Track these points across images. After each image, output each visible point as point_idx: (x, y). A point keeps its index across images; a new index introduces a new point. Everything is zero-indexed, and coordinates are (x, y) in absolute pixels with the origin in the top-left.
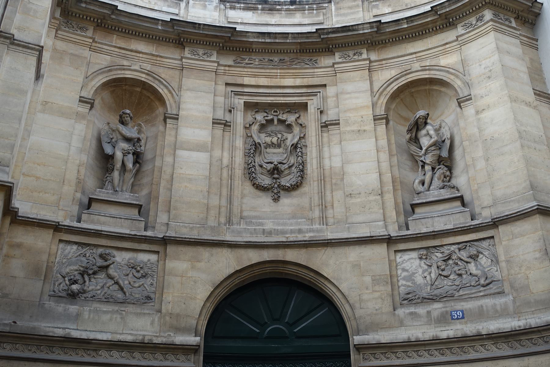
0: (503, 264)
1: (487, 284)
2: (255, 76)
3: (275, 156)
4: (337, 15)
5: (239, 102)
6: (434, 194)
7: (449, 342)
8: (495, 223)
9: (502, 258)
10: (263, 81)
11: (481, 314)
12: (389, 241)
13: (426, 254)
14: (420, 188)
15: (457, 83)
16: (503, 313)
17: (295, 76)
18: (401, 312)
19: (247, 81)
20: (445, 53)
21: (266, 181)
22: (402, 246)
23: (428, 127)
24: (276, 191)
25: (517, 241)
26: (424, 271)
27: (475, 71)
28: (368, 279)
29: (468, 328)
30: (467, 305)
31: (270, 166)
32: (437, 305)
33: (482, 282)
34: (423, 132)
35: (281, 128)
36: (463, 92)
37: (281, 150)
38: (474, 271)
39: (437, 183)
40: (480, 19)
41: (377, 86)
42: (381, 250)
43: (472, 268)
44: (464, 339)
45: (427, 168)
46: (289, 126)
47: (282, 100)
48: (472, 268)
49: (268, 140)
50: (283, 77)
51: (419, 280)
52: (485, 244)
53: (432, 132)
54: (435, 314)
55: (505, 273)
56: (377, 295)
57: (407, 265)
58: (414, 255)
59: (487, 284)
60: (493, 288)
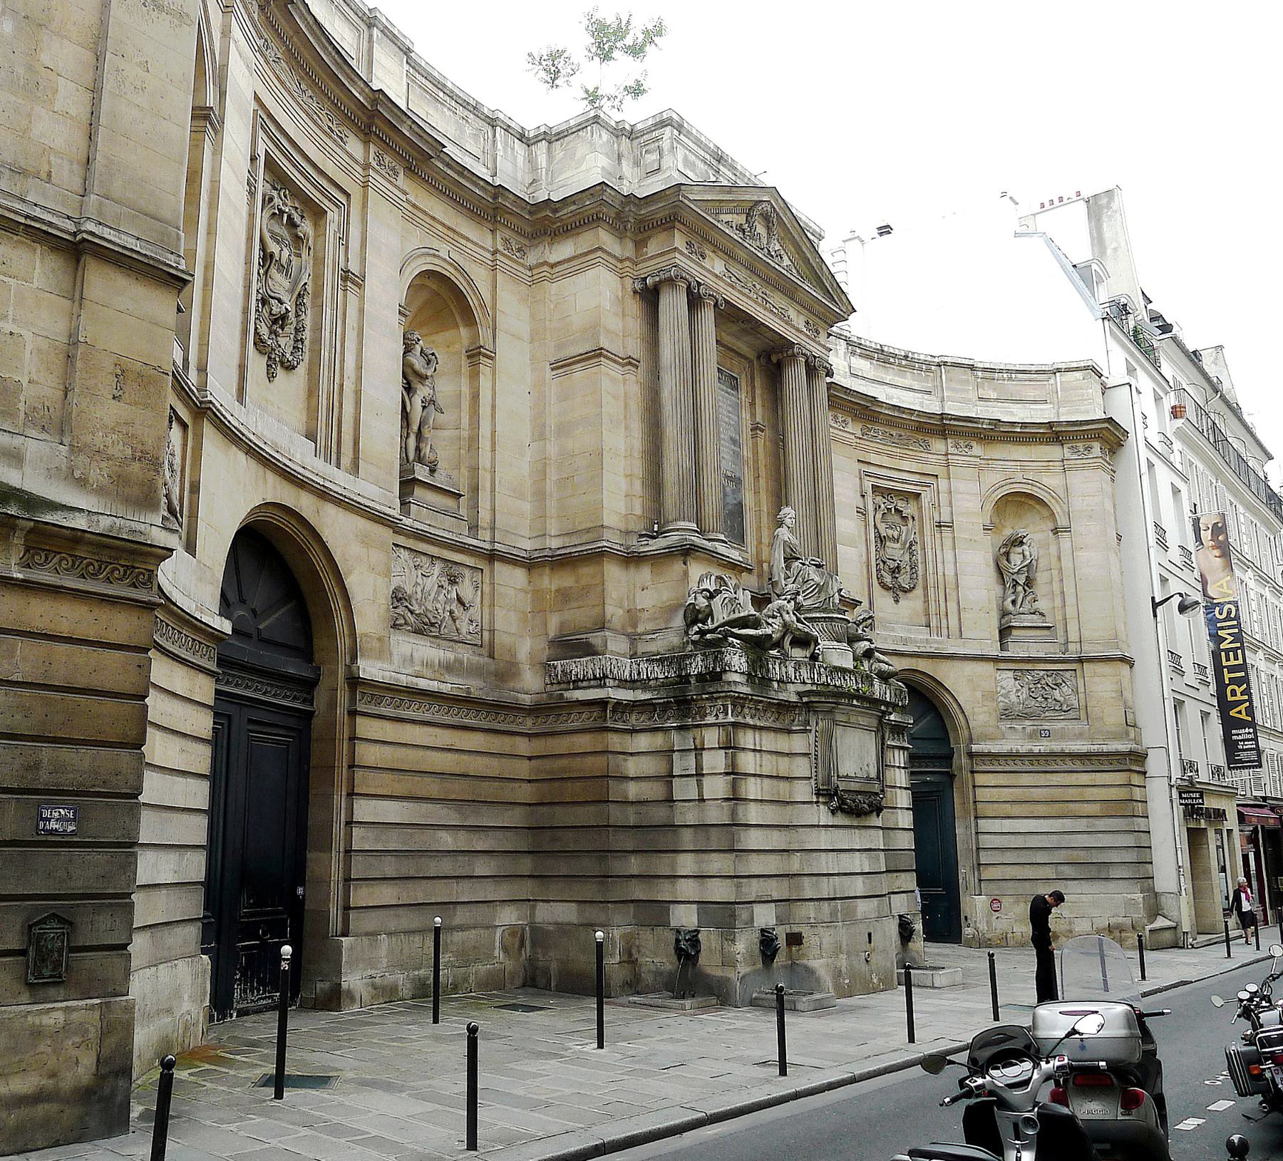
0: (1082, 696)
1: (1064, 710)
2: (878, 453)
3: (894, 550)
4: (948, 389)
5: (868, 485)
6: (1028, 620)
7: (1040, 755)
8: (1081, 661)
9: (1081, 690)
10: (886, 461)
11: (1063, 736)
12: (996, 660)
13: (1018, 675)
14: (1010, 607)
15: (1056, 509)
16: (1080, 736)
17: (913, 458)
18: (1004, 726)
19: (873, 458)
20: (1047, 469)
21: (888, 579)
22: (1003, 666)
23: (1025, 547)
24: (898, 592)
25: (1097, 679)
26: (1018, 691)
27: (1077, 504)
28: (979, 694)
29: (1056, 746)
30: (1047, 725)
31: (893, 565)
32: (1028, 723)
33: (1065, 708)
34: (1019, 550)
35: (897, 519)
36: (1062, 522)
37: (898, 545)
38: (1059, 698)
39: (1026, 607)
40: (1089, 449)
41: (984, 489)
42: (989, 668)
43: (1057, 694)
44: (1052, 755)
45: (1020, 588)
46: (905, 518)
47: (899, 486)
48: (1057, 694)
49: (890, 532)
50: (902, 458)
51: (1013, 698)
52: (1068, 674)
53: (1027, 553)
54: (1029, 729)
55: (1082, 703)
56: (985, 709)
57: (1004, 683)
58: (1011, 674)
59: (1064, 710)
60: (1072, 714)
